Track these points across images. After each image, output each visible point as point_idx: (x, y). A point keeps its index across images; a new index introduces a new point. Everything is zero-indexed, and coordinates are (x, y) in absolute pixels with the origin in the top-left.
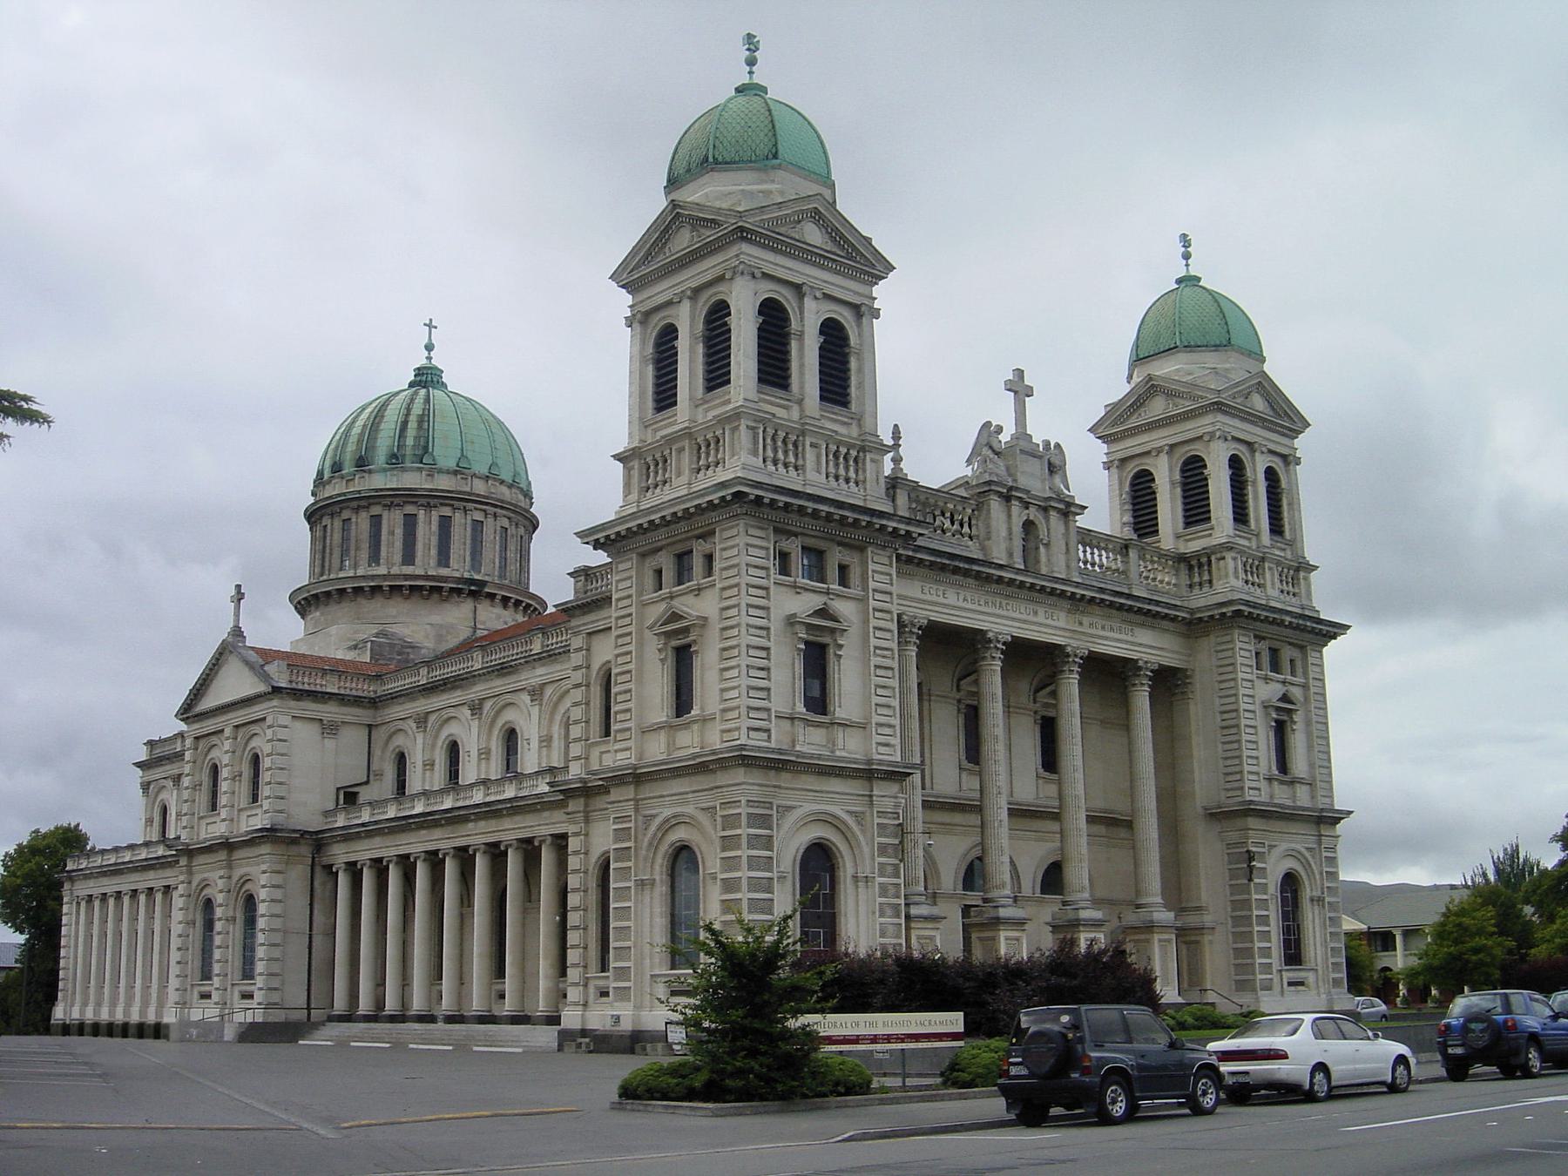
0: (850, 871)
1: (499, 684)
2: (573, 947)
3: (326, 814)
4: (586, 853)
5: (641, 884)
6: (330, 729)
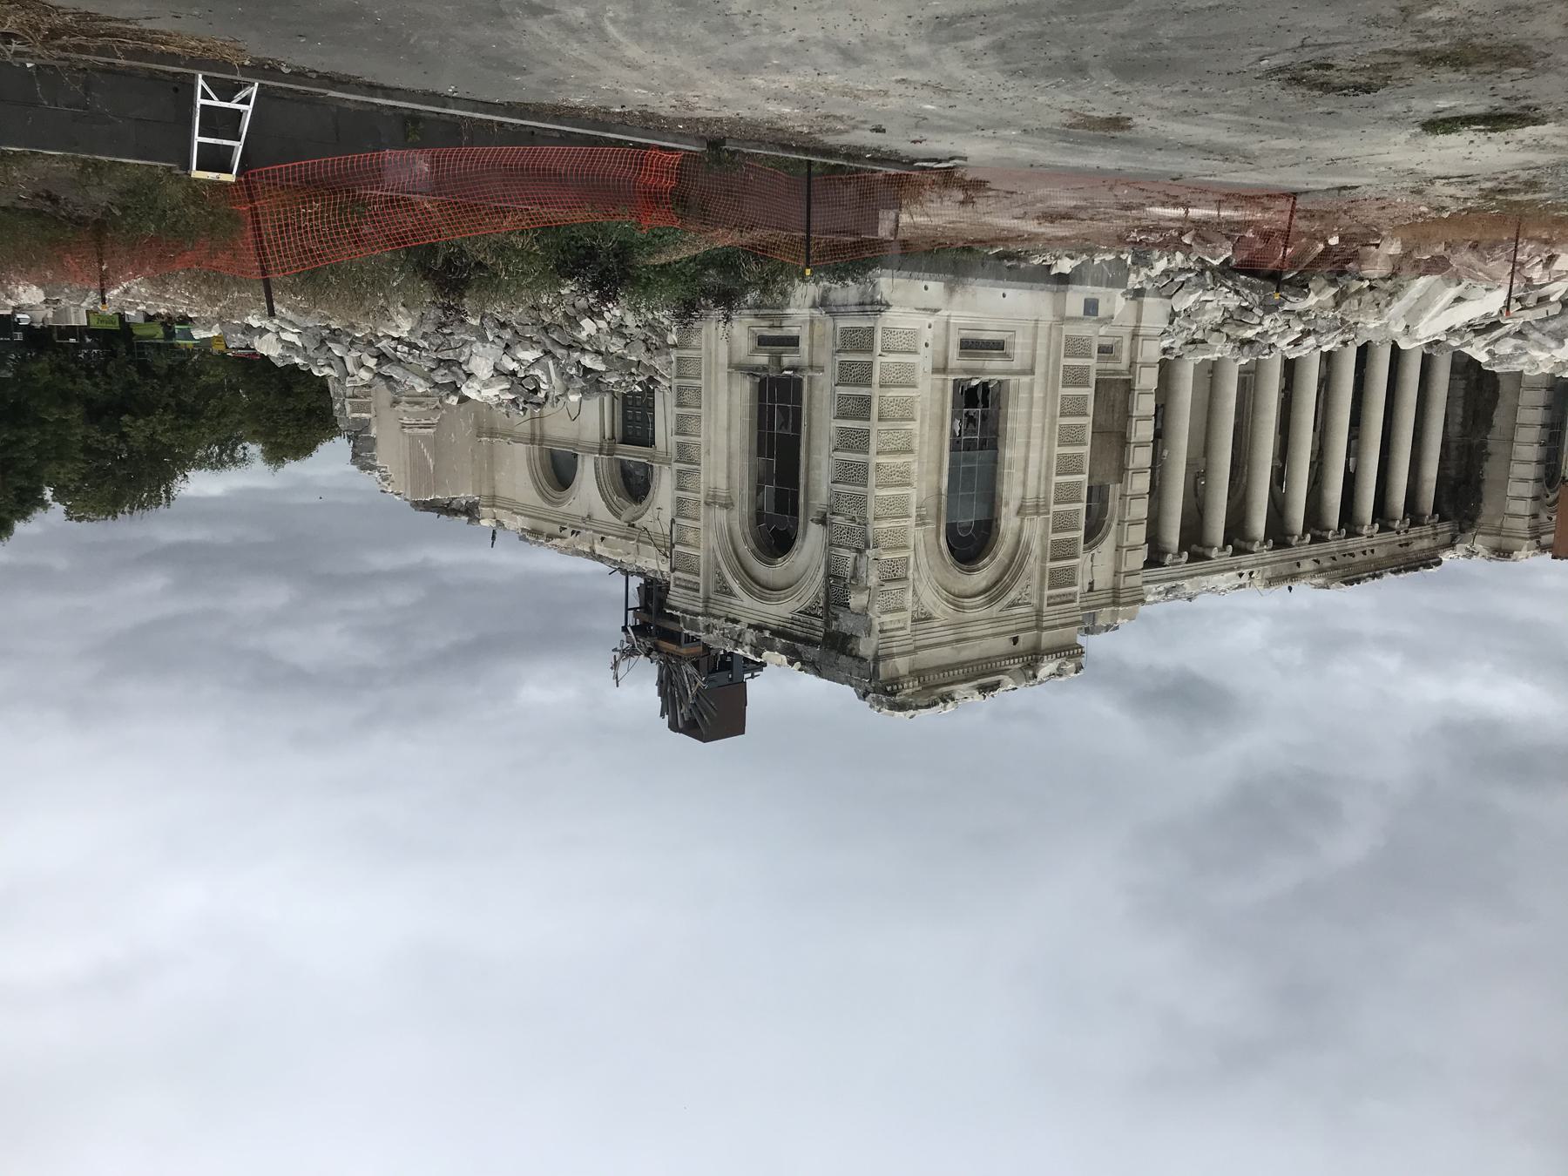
0: (736, 514)
2: (1147, 418)
4: (1118, 548)
5: (1038, 509)
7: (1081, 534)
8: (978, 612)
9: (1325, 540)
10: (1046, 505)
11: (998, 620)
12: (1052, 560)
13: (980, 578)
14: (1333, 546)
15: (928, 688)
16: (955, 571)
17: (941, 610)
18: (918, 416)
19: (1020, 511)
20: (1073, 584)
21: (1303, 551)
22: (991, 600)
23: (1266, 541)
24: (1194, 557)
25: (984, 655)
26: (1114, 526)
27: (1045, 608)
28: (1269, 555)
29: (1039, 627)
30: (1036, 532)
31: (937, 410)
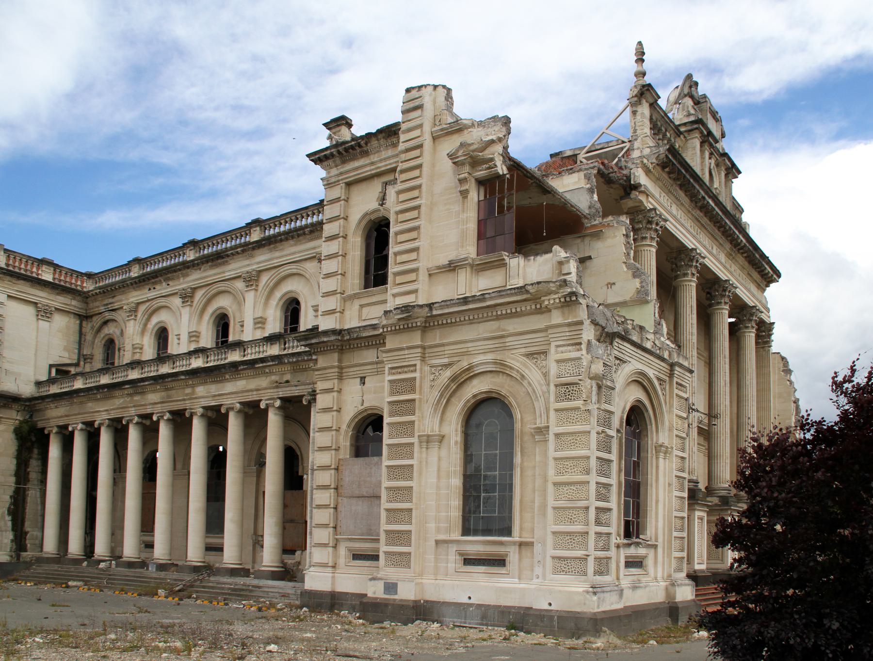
1: (210, 274)
3: (38, 384)
4: (339, 411)
5: (427, 440)
6: (44, 313)
7: (386, 420)
8: (482, 359)
9: (141, 416)
10: (420, 442)
11: (463, 354)
12: (414, 400)
13: (478, 387)
14: (133, 411)
15: (536, 299)
16: (504, 392)
17: (516, 360)
18: (550, 512)
19: (442, 438)
20: (390, 381)
21: (158, 408)
22: (468, 369)
23: (192, 415)
24: (255, 404)
25: (475, 326)
26: (344, 427)
27: (418, 363)
28: (187, 404)
29: (424, 348)
30: (426, 421)
31: (527, 516)
